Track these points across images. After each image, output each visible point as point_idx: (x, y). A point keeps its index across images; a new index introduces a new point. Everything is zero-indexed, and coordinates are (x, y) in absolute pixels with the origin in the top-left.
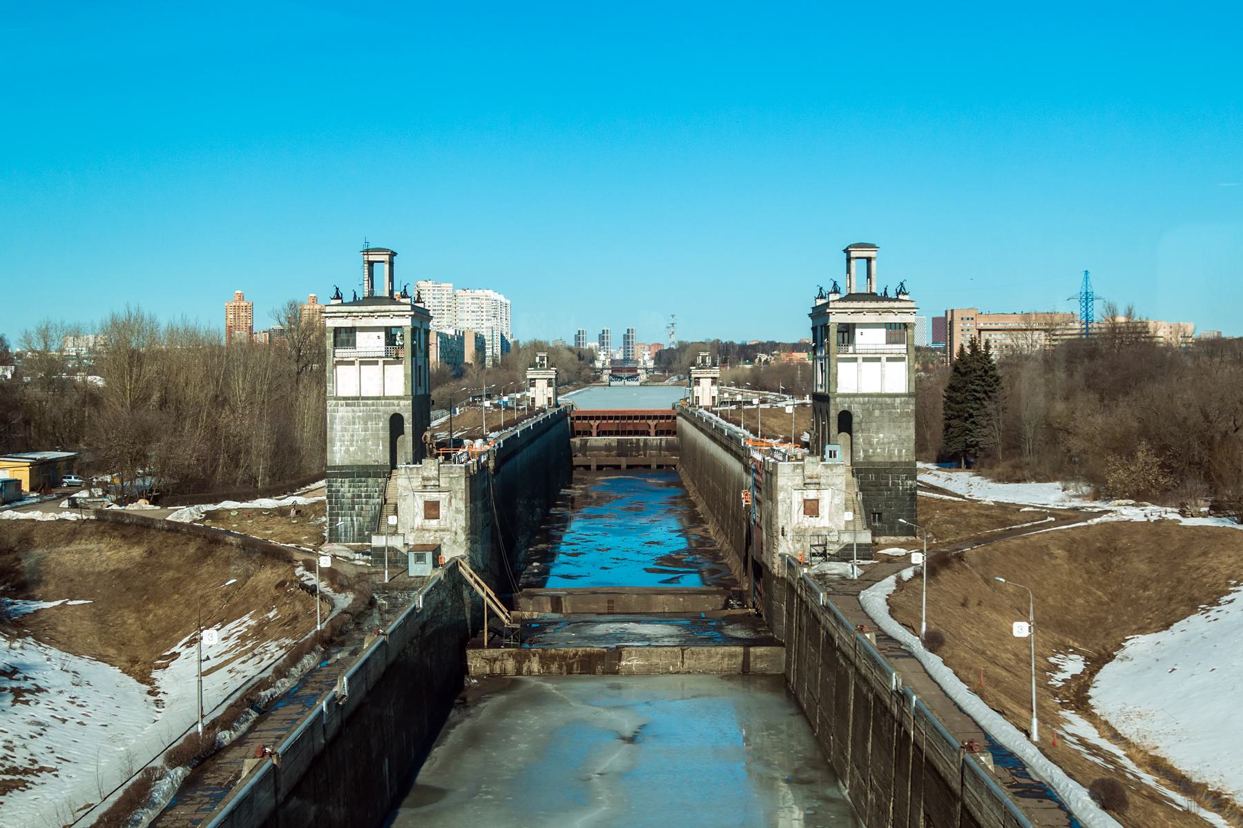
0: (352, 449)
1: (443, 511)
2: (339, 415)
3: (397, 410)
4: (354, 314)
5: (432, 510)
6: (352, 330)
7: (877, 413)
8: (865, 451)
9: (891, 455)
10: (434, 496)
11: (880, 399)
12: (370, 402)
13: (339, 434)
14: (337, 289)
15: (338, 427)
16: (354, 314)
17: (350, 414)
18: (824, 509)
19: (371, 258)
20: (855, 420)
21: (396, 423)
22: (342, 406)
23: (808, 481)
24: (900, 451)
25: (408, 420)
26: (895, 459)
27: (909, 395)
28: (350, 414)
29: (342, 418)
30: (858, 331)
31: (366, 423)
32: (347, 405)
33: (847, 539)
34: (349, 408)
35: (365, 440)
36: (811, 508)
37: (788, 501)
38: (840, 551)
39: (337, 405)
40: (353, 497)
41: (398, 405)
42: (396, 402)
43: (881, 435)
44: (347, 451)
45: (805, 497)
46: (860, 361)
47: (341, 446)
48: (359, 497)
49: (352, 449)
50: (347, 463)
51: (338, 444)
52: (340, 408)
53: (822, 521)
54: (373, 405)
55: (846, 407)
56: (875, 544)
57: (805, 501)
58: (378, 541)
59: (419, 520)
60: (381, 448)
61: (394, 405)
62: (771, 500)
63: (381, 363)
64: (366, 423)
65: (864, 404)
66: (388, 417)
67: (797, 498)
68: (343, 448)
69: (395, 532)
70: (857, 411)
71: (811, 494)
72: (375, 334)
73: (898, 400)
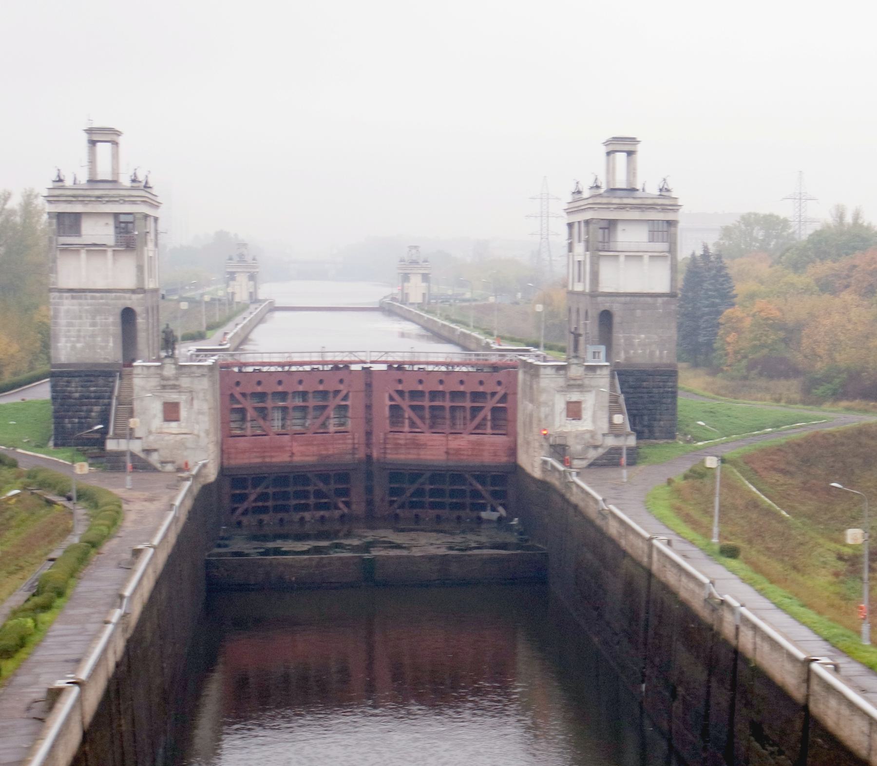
0: (79, 345)
1: (183, 413)
2: (63, 309)
3: (128, 304)
4: (80, 199)
5: (171, 412)
6: (78, 216)
7: (638, 312)
8: (627, 352)
9: (652, 353)
10: (173, 397)
11: (642, 299)
12: (98, 295)
13: (64, 329)
14: (59, 170)
15: (63, 321)
16: (80, 199)
17: (76, 308)
18: (587, 414)
19: (95, 138)
20: (616, 320)
21: (128, 316)
22: (67, 298)
23: (572, 382)
24: (661, 352)
25: (298, 368)
26: (656, 361)
27: (672, 295)
28: (76, 308)
29: (68, 311)
30: (620, 227)
31: (94, 317)
32: (73, 298)
33: (611, 442)
34: (75, 301)
35: (93, 336)
36: (574, 411)
37: (550, 403)
38: (604, 455)
39: (61, 298)
40: (81, 398)
41: (130, 299)
42: (127, 295)
43: (643, 336)
44: (73, 348)
45: (568, 399)
46: (622, 258)
47: (66, 342)
48: (88, 398)
49: (79, 345)
50: (73, 360)
51: (63, 340)
52: (66, 302)
53: (585, 425)
54: (102, 298)
55: (607, 307)
56: (637, 447)
57: (568, 403)
58: (111, 445)
59: (157, 422)
60: (111, 344)
61: (125, 298)
62: (532, 401)
63: (110, 254)
64: (94, 317)
65: (625, 304)
66: (118, 311)
67: (560, 403)
68: (69, 345)
69: (131, 435)
70: (616, 308)
71: (575, 397)
72: (102, 222)
73: (660, 300)
